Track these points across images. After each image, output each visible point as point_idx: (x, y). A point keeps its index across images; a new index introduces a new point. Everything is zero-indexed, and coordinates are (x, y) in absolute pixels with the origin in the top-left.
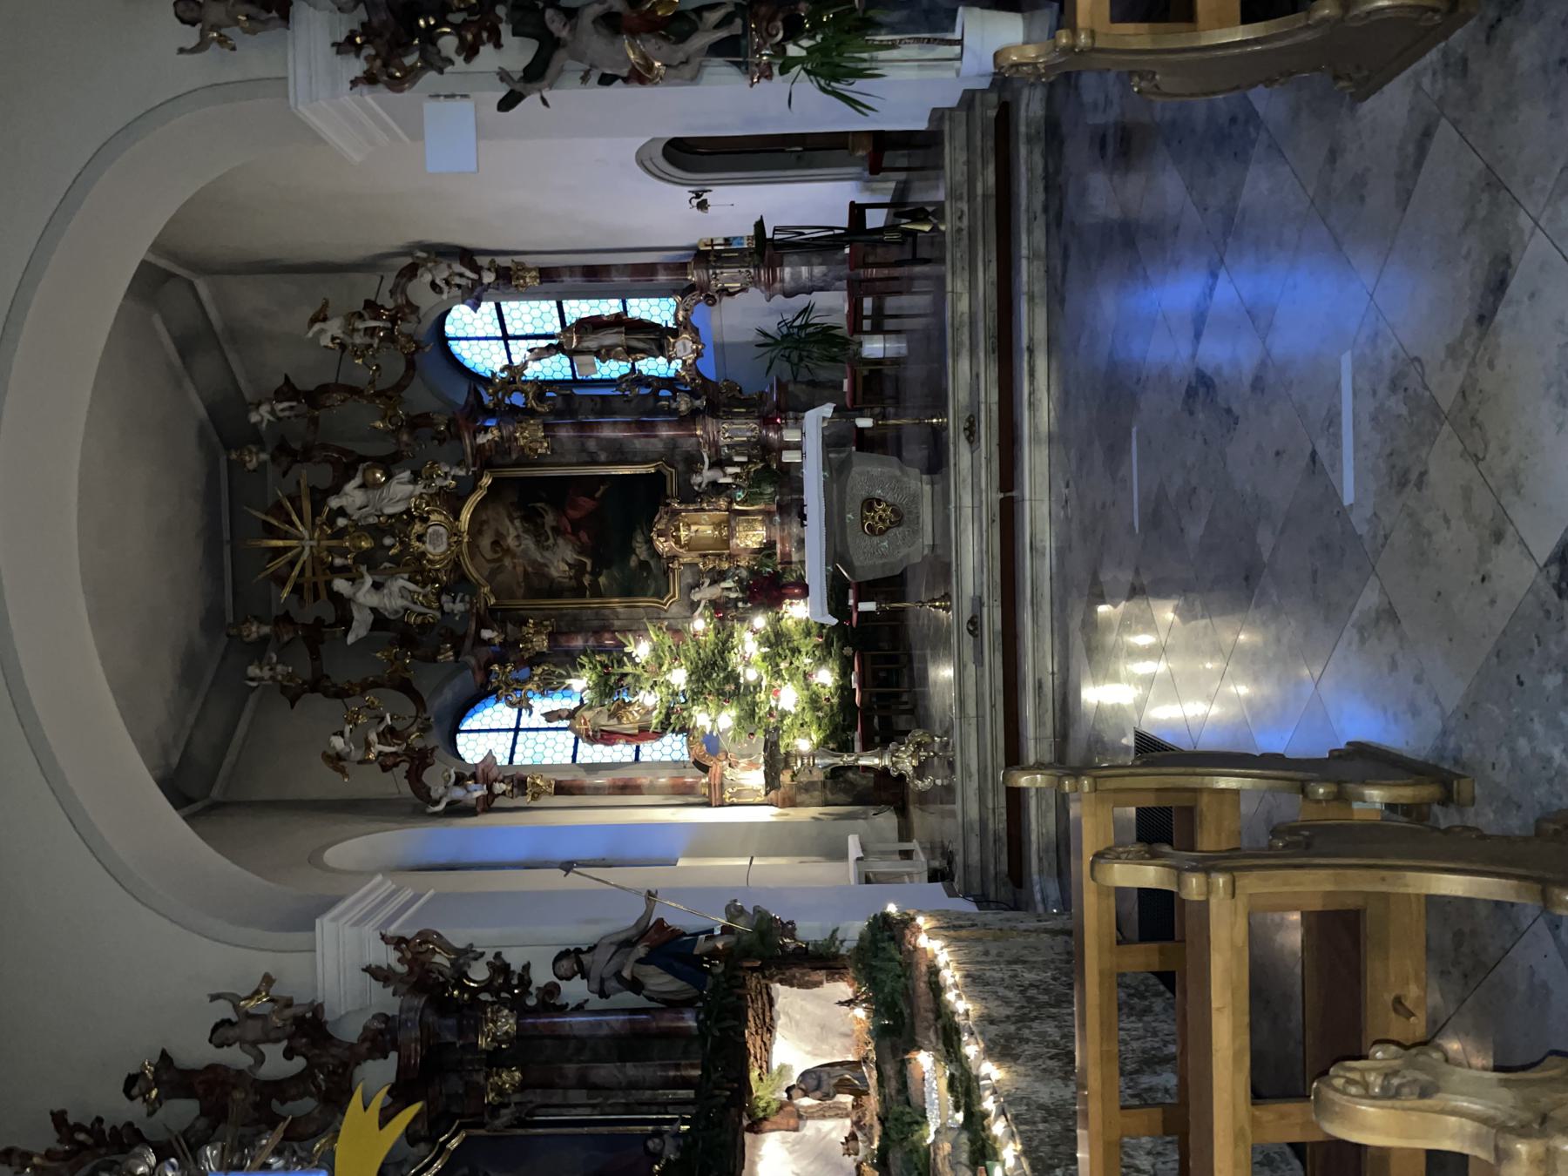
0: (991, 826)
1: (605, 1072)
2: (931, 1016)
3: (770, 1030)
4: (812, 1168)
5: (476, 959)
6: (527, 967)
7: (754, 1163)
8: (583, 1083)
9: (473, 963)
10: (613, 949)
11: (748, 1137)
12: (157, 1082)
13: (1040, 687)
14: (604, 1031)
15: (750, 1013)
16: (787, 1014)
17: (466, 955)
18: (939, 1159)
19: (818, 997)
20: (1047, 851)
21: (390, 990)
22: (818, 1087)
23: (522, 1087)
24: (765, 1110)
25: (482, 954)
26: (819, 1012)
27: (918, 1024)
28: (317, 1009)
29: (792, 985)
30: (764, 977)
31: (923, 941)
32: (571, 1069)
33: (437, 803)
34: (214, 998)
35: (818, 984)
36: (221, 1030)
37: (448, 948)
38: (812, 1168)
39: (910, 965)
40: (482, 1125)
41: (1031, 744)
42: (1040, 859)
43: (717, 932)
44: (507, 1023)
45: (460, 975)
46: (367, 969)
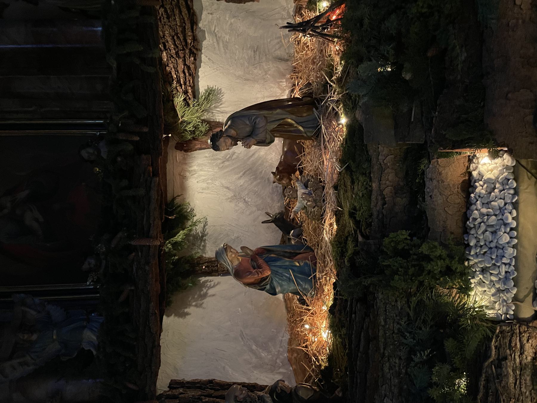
4: (242, 182)
7: (183, 178)
18: (509, 368)
24: (193, 132)
38: (242, 182)
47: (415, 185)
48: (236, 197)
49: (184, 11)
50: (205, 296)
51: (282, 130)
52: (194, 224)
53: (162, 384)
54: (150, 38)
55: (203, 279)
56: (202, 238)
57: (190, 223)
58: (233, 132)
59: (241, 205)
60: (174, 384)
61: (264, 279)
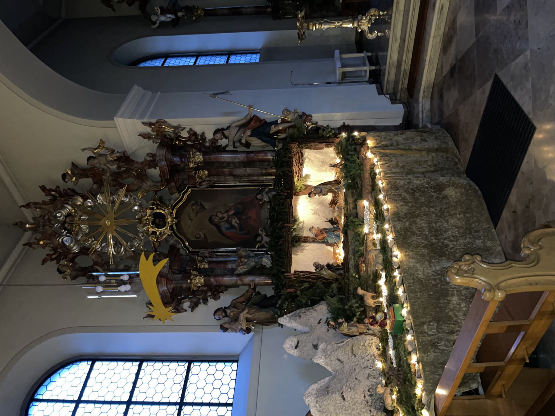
0: (403, 68)
1: (239, 171)
2: (370, 188)
3: (302, 164)
4: (317, 207)
5: (182, 130)
6: (203, 134)
7: (296, 206)
8: (231, 174)
9: (182, 132)
10: (237, 129)
11: (294, 197)
12: (74, 174)
13: (442, 9)
14: (237, 160)
15: (294, 159)
16: (309, 158)
17: (177, 128)
18: (368, 241)
19: (322, 152)
20: (428, 87)
21: (151, 141)
22: (321, 192)
23: (209, 175)
25: (184, 128)
26: (321, 157)
27: (364, 189)
28: (124, 152)
29: (311, 149)
30: (299, 147)
31: (369, 155)
32: (226, 170)
33: (154, 23)
34: (84, 150)
35: (322, 148)
36: (90, 161)
37: (170, 126)
38: (317, 207)
39: (362, 164)
40: (196, 187)
41: (431, 39)
42: (424, 92)
43: (279, 121)
44: (199, 157)
45: (178, 138)
46: (140, 135)
47: (356, 207)
48: (315, 213)
49: (300, 154)
50: (304, 249)
51: (330, 191)
52: (300, 223)
53: (292, 272)
54: (290, 164)
55: (303, 244)
56: (302, 228)
57: (297, 223)
58: (315, 192)
59: (317, 216)
60: (295, 271)
61: (324, 238)
